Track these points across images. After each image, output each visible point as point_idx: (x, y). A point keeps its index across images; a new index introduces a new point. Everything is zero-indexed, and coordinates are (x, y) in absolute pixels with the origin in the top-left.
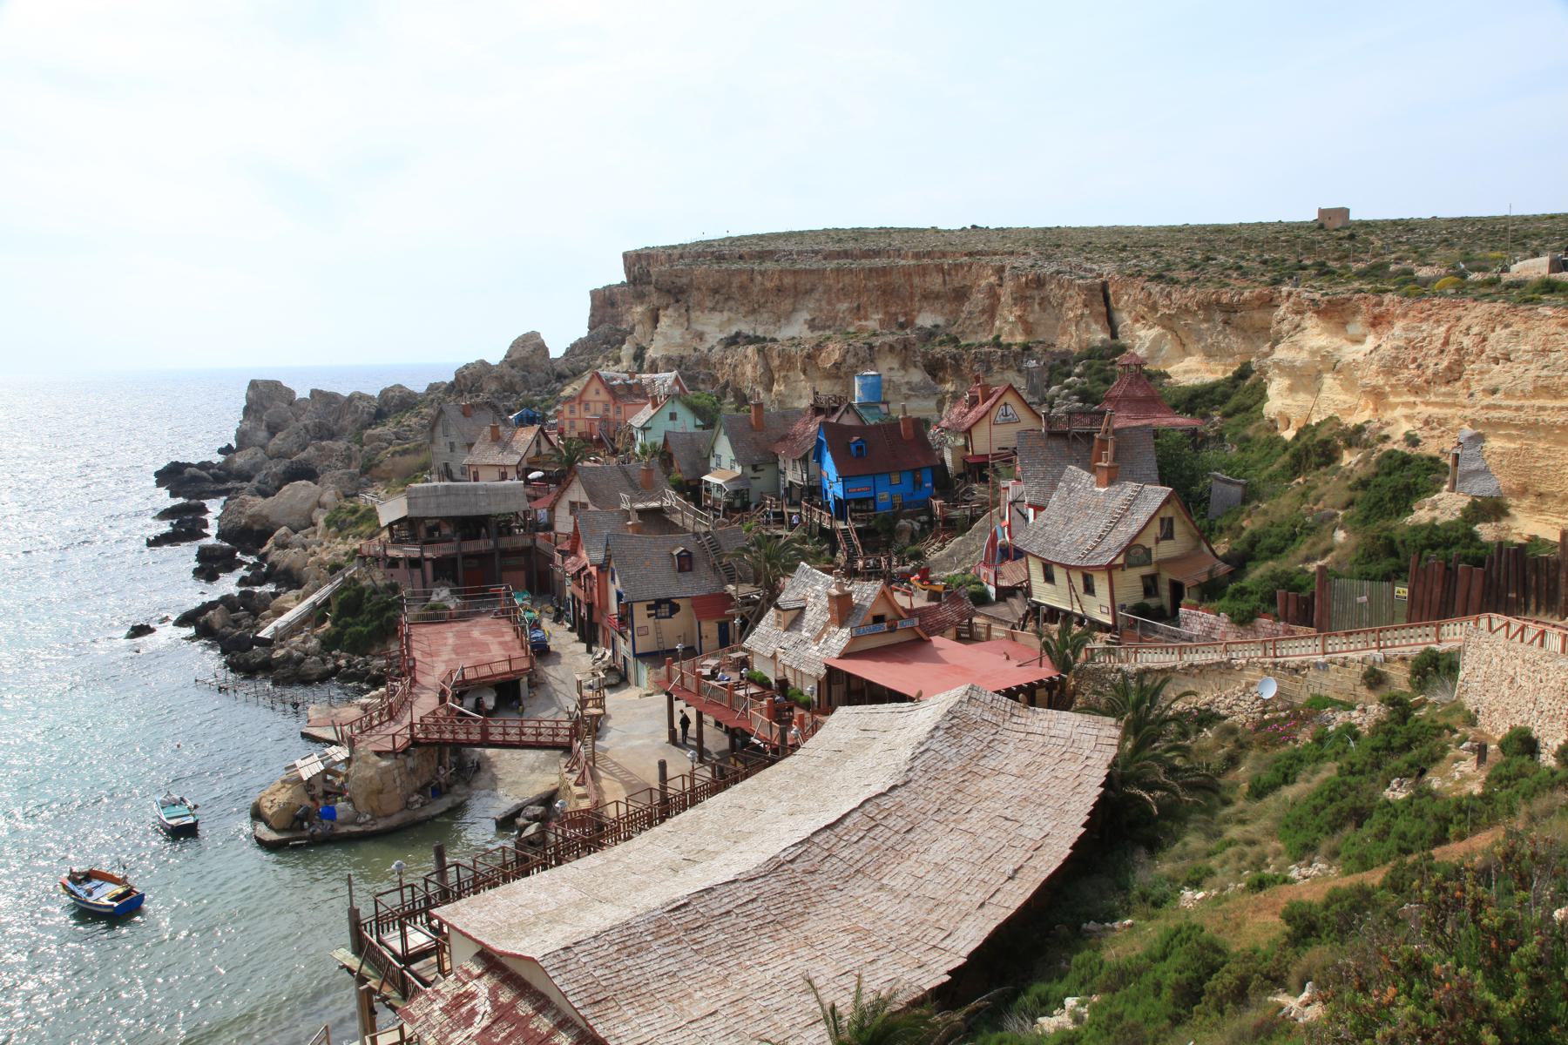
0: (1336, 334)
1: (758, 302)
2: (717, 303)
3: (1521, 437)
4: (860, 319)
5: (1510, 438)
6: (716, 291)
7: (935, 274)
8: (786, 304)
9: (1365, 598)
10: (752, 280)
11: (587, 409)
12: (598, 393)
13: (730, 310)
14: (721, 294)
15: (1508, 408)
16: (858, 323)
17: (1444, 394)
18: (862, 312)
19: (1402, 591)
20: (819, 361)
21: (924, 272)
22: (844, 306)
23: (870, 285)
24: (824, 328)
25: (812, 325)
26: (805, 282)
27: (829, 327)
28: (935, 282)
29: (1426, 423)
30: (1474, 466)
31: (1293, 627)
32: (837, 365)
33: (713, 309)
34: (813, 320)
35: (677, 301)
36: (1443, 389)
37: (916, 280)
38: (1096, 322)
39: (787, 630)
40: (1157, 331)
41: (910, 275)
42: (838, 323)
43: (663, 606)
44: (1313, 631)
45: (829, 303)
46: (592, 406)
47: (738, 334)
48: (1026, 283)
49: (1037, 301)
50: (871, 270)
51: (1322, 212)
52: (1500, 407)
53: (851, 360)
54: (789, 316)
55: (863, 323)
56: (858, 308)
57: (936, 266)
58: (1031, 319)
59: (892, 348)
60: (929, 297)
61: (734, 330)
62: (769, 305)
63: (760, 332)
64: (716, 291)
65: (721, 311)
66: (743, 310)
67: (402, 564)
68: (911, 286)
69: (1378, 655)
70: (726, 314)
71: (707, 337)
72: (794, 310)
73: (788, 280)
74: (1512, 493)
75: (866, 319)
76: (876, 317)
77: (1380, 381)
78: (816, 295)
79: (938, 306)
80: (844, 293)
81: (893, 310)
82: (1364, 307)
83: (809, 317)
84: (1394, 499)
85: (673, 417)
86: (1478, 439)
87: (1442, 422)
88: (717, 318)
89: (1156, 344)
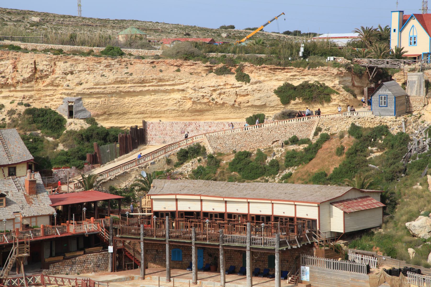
3: (104, 97)
5: (97, 98)
9: (109, 150)
15: (99, 88)
17: (28, 87)
19: (118, 145)
29: (24, 98)
30: (80, 109)
31: (94, 165)
36: (26, 85)
39: (6, 206)
44: (99, 164)
52: (96, 88)
69: (167, 154)
74: (98, 115)
84: (57, 124)
86: (80, 99)
87: (31, 97)
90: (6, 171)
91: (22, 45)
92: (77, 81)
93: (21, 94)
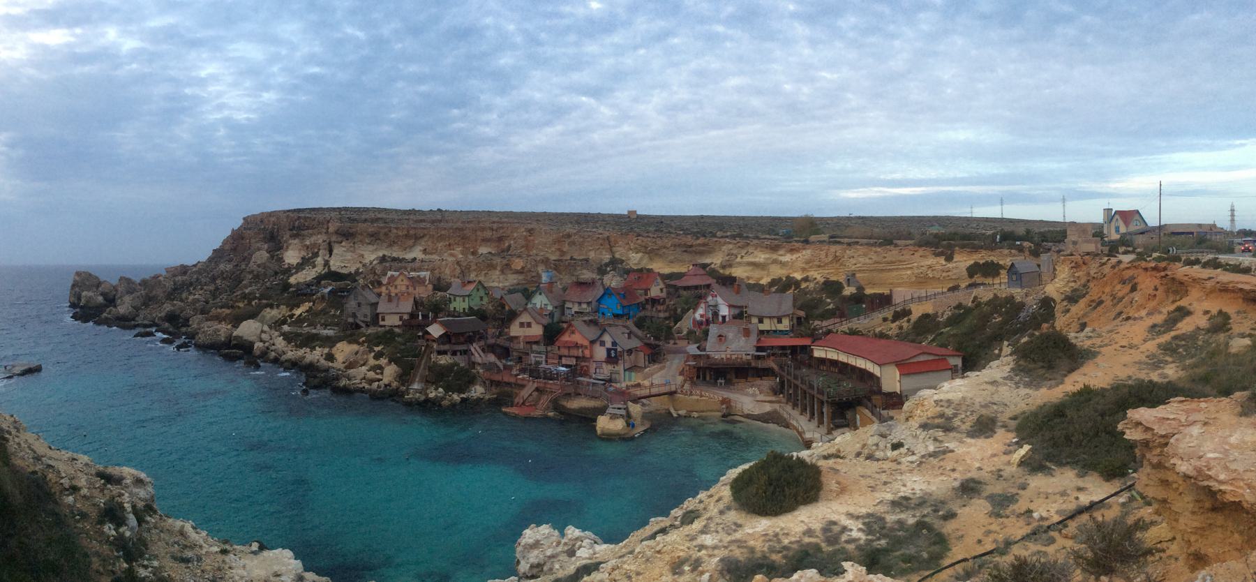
0: (773, 253)
1: (394, 242)
2: (372, 240)
4: (451, 250)
6: (372, 236)
7: (488, 231)
8: (411, 242)
10: (390, 231)
11: (396, 287)
12: (402, 281)
13: (378, 244)
14: (375, 238)
16: (449, 252)
18: (452, 247)
20: (512, 266)
21: (483, 229)
22: (440, 245)
23: (455, 235)
24: (431, 254)
25: (425, 251)
26: (420, 233)
27: (434, 253)
28: (488, 234)
32: (523, 268)
33: (369, 244)
34: (425, 250)
35: (347, 240)
37: (479, 233)
38: (606, 252)
40: (640, 255)
41: (476, 231)
42: (439, 251)
43: (630, 352)
45: (433, 242)
46: (399, 287)
47: (384, 256)
48: (563, 236)
49: (567, 242)
50: (456, 229)
51: (629, 212)
53: (529, 266)
54: (411, 247)
55: (452, 251)
56: (450, 245)
57: (489, 227)
58: (565, 250)
59: (543, 261)
60: (485, 241)
61: (381, 254)
62: (399, 243)
63: (395, 255)
64: (372, 236)
65: (373, 245)
66: (385, 245)
67: (459, 354)
68: (476, 236)
70: (375, 247)
71: (366, 256)
72: (414, 246)
73: (412, 232)
75: (453, 250)
76: (458, 249)
77: (803, 265)
78: (425, 239)
79: (489, 244)
80: (441, 238)
81: (467, 246)
82: (787, 246)
83: (422, 249)
85: (478, 290)
88: (371, 248)
89: (641, 259)
90: (776, 321)
91: (842, 240)
92: (854, 262)
93: (827, 271)
